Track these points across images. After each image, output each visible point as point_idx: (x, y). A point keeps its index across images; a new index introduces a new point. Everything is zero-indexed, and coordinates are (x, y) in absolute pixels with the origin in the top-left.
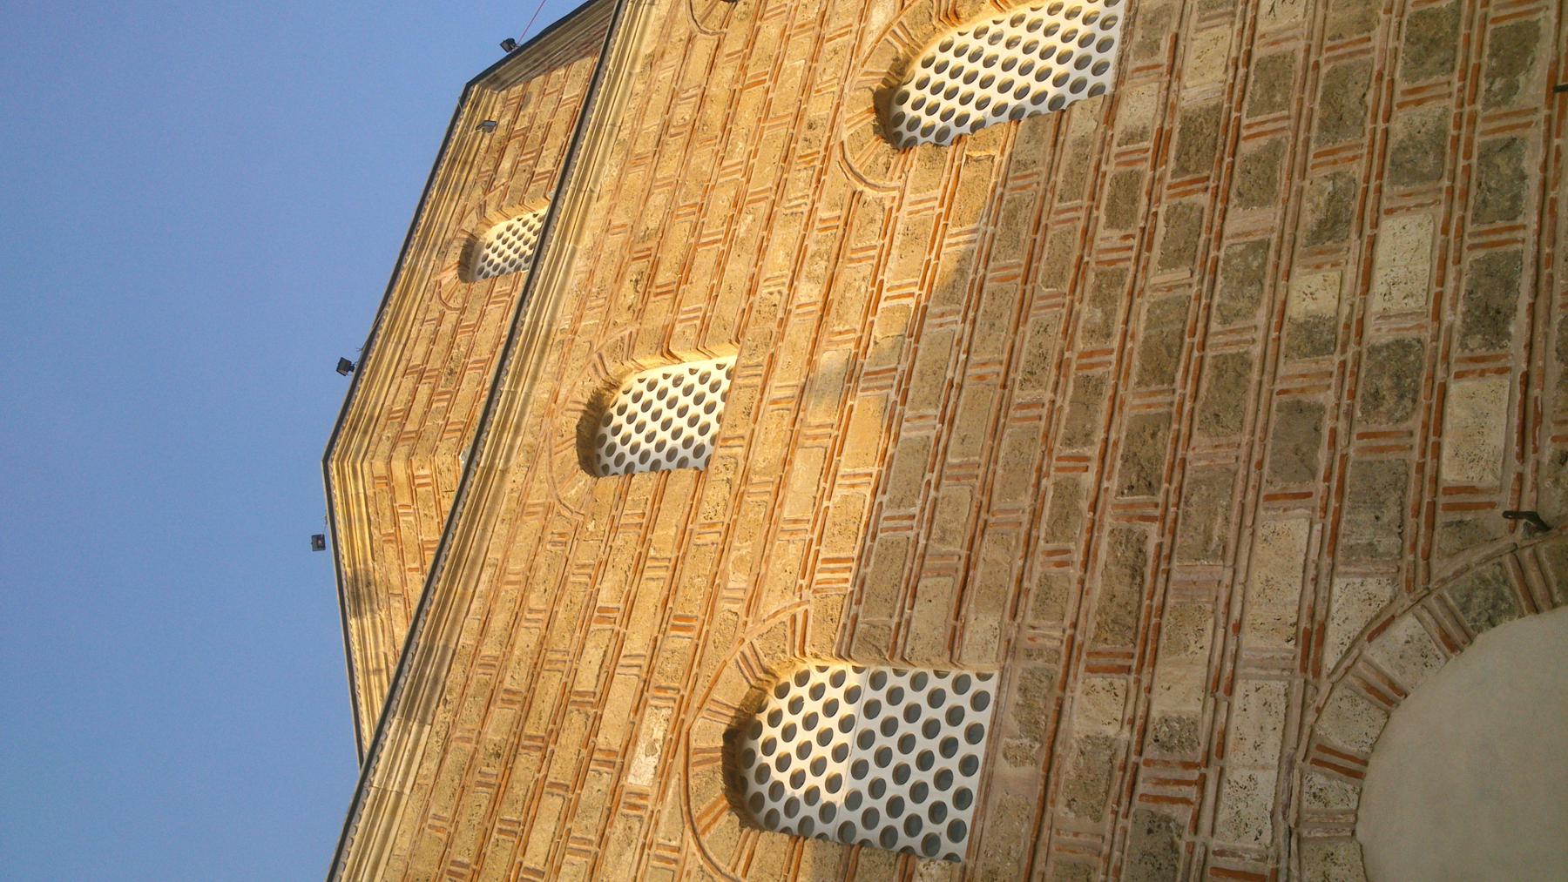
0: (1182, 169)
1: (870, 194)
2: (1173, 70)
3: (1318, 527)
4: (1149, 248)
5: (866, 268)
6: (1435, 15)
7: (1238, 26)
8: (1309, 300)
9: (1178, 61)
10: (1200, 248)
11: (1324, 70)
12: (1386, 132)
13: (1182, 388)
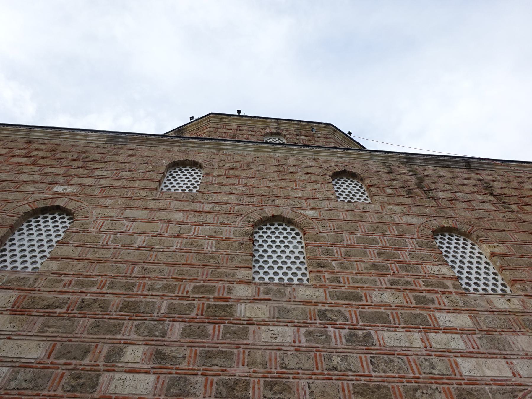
0: (209, 306)
3: (33, 361)
4: (179, 299)
6: (246, 389)
7: (267, 320)
8: (132, 352)
9: (257, 301)
10: (173, 315)
11: (235, 351)
12: (197, 374)
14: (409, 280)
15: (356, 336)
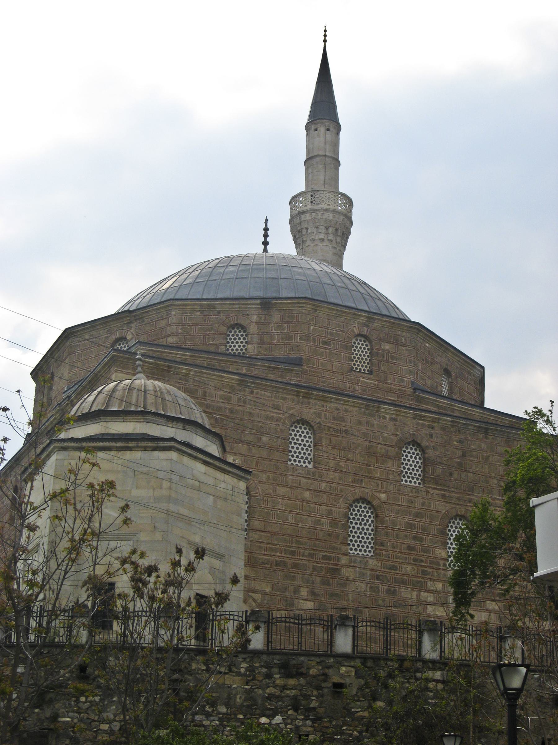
1: (341, 500)
2: (349, 566)
5: (325, 501)
13: (291, 570)
14: (423, 559)
15: (390, 590)
